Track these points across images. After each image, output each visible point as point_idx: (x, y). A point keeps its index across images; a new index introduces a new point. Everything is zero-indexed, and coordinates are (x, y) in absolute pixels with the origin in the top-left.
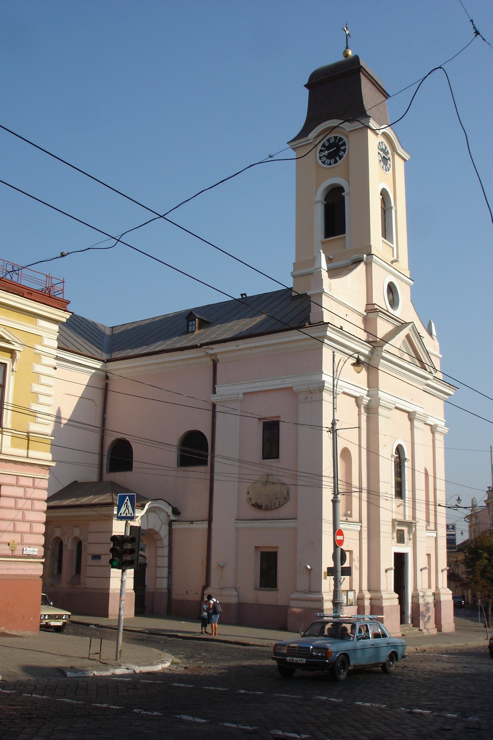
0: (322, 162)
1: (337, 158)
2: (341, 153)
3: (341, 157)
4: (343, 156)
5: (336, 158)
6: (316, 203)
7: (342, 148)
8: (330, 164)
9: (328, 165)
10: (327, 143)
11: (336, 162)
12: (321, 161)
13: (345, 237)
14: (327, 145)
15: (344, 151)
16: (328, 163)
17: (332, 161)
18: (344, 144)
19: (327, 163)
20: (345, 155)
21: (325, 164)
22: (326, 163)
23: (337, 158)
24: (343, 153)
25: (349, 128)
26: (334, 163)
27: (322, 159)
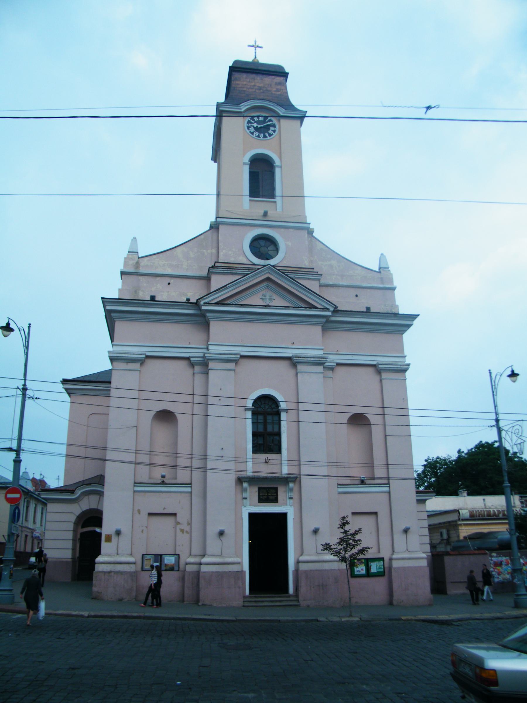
0: (250, 132)
1: (267, 135)
2: (271, 132)
3: (270, 135)
4: (272, 135)
5: (266, 134)
6: (245, 164)
7: (272, 128)
8: (259, 136)
9: (256, 136)
10: (256, 119)
11: (265, 137)
12: (249, 131)
13: (275, 202)
14: (256, 120)
15: (274, 131)
16: (257, 135)
17: (261, 135)
18: (274, 126)
19: (255, 135)
20: (275, 134)
21: (253, 135)
22: (254, 134)
23: (267, 135)
24: (272, 132)
25: (284, 113)
26: (263, 138)
27: (250, 129)
